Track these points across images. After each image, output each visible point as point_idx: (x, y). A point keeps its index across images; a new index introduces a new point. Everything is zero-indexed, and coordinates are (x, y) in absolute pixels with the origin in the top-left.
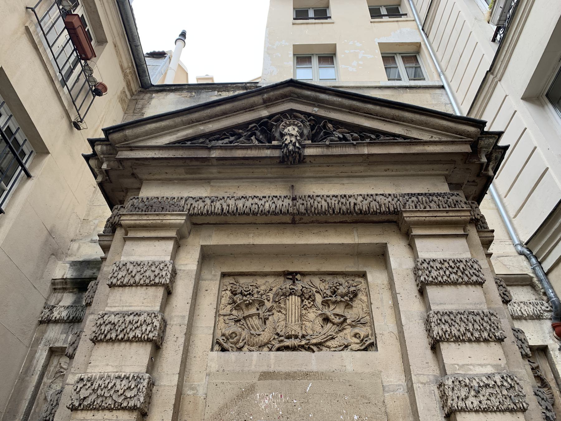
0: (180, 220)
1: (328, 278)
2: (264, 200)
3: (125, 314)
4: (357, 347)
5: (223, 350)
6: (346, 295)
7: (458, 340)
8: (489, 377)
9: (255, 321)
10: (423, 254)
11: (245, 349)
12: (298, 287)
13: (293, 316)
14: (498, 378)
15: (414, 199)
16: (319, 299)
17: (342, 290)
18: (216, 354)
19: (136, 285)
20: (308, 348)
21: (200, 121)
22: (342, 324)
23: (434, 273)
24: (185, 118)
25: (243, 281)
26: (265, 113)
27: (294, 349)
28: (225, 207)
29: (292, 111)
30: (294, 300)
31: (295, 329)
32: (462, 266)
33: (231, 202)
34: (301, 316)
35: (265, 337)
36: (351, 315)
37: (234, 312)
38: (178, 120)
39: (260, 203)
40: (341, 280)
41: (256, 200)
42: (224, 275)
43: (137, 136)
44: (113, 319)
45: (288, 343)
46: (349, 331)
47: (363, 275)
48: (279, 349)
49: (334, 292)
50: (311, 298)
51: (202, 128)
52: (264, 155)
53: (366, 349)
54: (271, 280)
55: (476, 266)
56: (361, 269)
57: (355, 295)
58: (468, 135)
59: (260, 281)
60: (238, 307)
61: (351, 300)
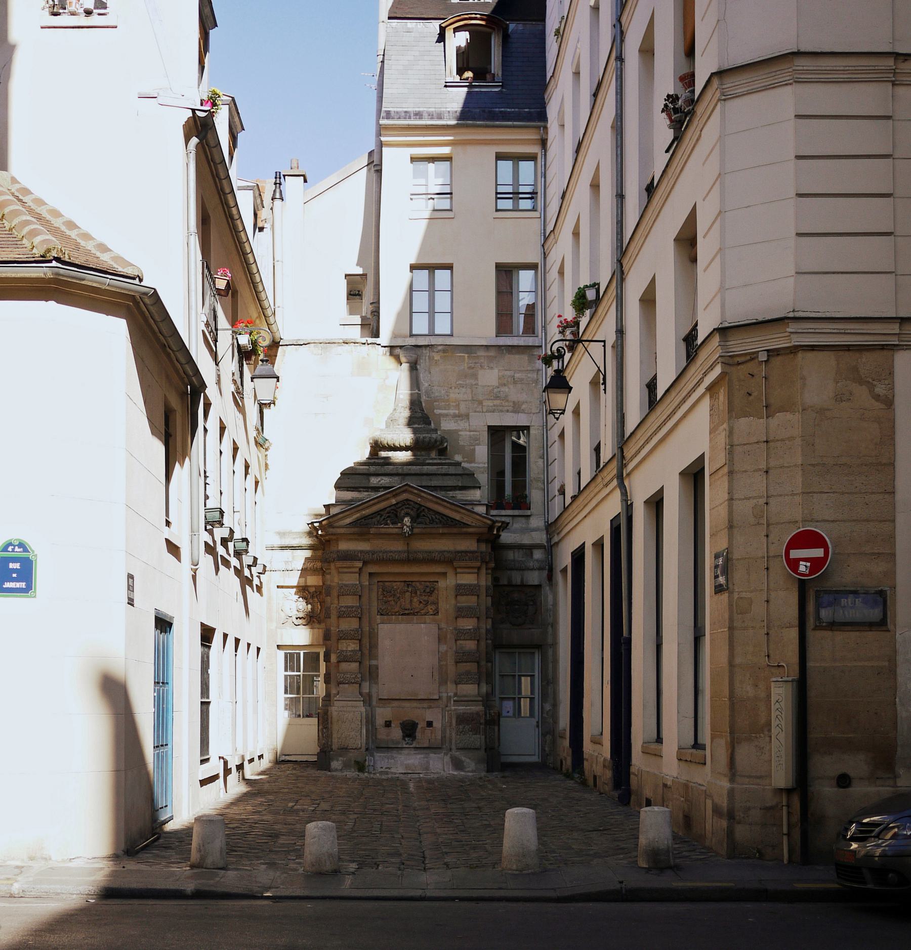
0: (360, 564)
1: (423, 583)
2: (396, 553)
3: (347, 607)
4: (432, 613)
5: (382, 615)
6: (429, 592)
7: (463, 617)
8: (469, 629)
9: (393, 603)
10: (459, 582)
11: (390, 614)
12: (410, 589)
13: (408, 601)
14: (472, 631)
15: (460, 554)
16: (418, 593)
17: (428, 590)
18: (378, 617)
19: (348, 595)
20: (414, 614)
21: (362, 510)
22: (426, 605)
23: (461, 591)
24: (355, 510)
25: (387, 584)
26: (394, 501)
27: (408, 614)
28: (378, 558)
29: (407, 500)
30: (408, 594)
31: (408, 606)
32: (472, 588)
33: (381, 554)
34: (411, 600)
35: (396, 610)
36: (431, 599)
37: (384, 598)
38: (353, 511)
39: (394, 555)
40: (428, 584)
41: (392, 554)
42: (378, 582)
43: (335, 521)
44: (343, 609)
45: (406, 612)
46: (429, 607)
47: (437, 582)
48: (402, 615)
49: (424, 591)
50: (416, 593)
51: (364, 512)
52: (394, 532)
53: (435, 615)
54: (398, 583)
55: (477, 588)
56: (436, 580)
57: (433, 591)
58: (488, 524)
59: (394, 584)
60: (386, 597)
61: (431, 594)
